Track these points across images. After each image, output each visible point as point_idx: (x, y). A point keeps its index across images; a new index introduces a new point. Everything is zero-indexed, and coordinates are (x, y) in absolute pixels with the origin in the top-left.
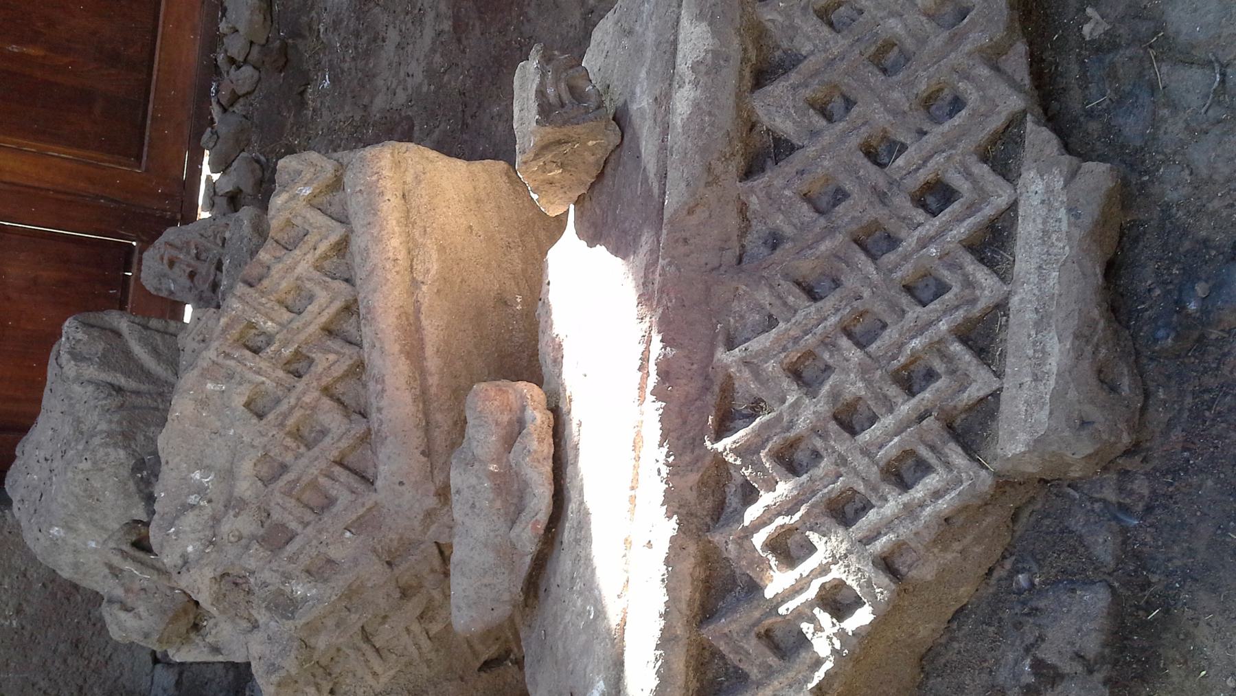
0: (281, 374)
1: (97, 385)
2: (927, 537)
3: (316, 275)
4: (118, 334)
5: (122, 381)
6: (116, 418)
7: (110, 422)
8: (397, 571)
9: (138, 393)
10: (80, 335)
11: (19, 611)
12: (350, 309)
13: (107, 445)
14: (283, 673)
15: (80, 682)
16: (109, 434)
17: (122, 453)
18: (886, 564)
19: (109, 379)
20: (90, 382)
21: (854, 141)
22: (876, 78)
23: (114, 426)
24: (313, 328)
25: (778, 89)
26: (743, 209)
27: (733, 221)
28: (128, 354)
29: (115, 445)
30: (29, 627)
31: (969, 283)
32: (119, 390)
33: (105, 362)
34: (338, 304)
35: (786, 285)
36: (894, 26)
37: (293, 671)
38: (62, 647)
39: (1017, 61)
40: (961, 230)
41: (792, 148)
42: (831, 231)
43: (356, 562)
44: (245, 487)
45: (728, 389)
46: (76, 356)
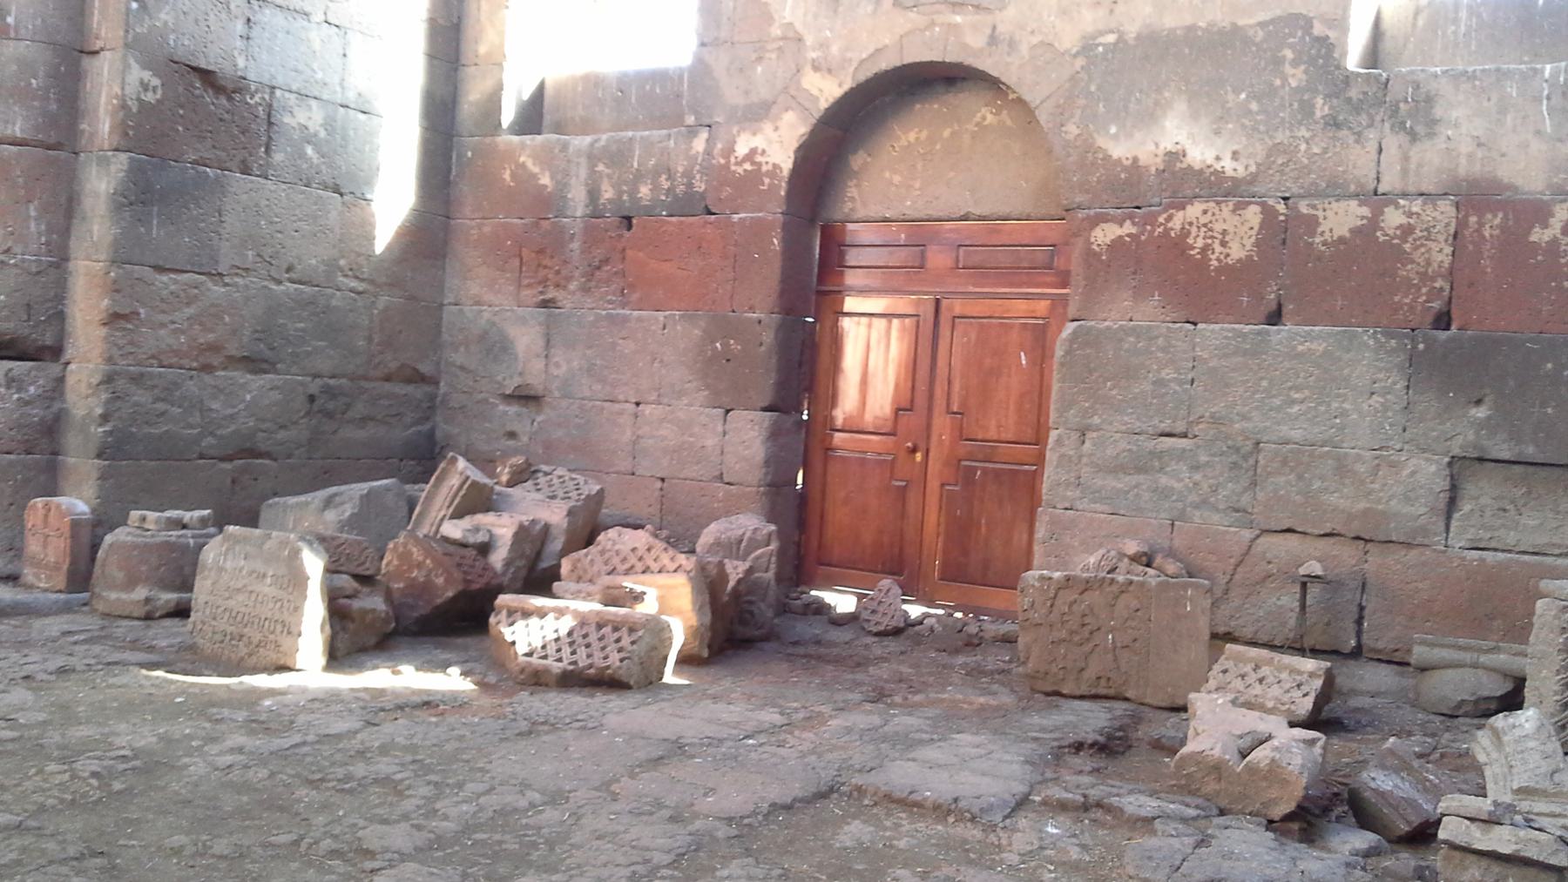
5: (744, 544)
9: (738, 549)
33: (750, 539)
44: (617, 547)
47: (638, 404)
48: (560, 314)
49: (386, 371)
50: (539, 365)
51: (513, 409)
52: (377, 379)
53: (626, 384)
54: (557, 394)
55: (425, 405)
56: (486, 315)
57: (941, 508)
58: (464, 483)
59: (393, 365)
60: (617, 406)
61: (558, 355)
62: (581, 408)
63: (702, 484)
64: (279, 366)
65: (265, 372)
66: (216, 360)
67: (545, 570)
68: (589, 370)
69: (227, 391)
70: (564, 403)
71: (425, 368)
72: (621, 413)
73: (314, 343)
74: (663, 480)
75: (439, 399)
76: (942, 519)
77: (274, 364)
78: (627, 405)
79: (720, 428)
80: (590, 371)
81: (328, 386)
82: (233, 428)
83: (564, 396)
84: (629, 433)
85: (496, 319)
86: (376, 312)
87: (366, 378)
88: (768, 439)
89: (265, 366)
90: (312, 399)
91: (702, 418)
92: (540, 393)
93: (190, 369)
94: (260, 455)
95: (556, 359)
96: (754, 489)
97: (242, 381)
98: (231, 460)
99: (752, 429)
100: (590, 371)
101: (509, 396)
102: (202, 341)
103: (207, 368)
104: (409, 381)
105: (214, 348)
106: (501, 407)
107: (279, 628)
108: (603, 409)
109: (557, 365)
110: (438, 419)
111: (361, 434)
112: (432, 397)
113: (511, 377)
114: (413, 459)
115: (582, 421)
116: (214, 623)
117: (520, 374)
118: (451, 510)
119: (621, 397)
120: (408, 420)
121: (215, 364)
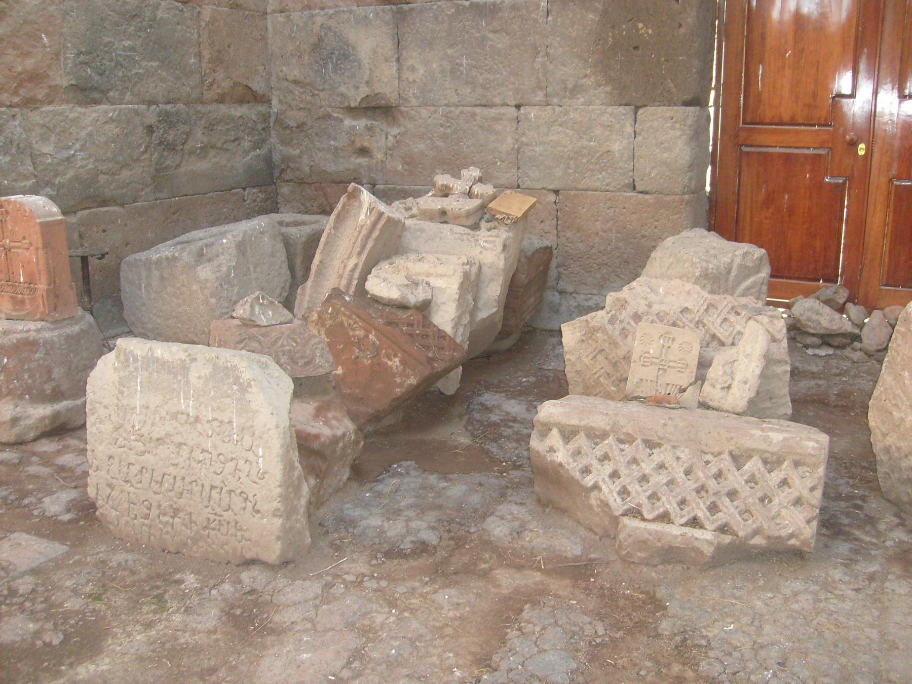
0: (697, 319)
1: (731, 264)
2: (602, 497)
3: (735, 332)
4: (758, 272)
5: (734, 273)
6: (714, 271)
7: (712, 269)
8: (622, 361)
9: (727, 280)
10: (756, 256)
11: (643, 236)
12: (723, 344)
13: (702, 268)
14: (590, 321)
15: (609, 264)
16: (707, 269)
17: (697, 274)
18: (596, 487)
19: (734, 268)
20: (732, 261)
21: (737, 486)
22: (759, 494)
23: (710, 271)
24: (714, 331)
25: (760, 464)
26: (720, 454)
27: (716, 449)
28: (748, 276)
29: (702, 271)
30: (635, 241)
31: (682, 517)
32: (729, 272)
33: (742, 267)
34: (723, 339)
35: (690, 462)
36: (776, 501)
37: (590, 325)
38: (625, 255)
39: (758, 541)
40: (700, 514)
41: (738, 469)
42: (707, 477)
43: (626, 345)
44: (656, 308)
45: (659, 445)
46: (745, 255)
47: (518, 107)
48: (412, 9)
49: (219, 91)
50: (388, 71)
51: (361, 124)
52: (212, 102)
53: (502, 85)
54: (414, 102)
55: (260, 127)
56: (319, 20)
57: (888, 207)
58: (374, 225)
59: (227, 84)
60: (493, 112)
61: (413, 58)
62: (447, 117)
63: (609, 194)
64: (111, 94)
65: (97, 102)
66: (41, 94)
67: (484, 320)
68: (452, 72)
69: (58, 130)
70: (424, 113)
71: (257, 85)
72: (498, 119)
73: (144, 63)
74: (556, 192)
75: (272, 119)
76: (889, 219)
77: (104, 92)
78: (503, 110)
79: (629, 129)
80: (454, 71)
81: (168, 114)
82: (71, 173)
83: (424, 104)
84: (510, 140)
85: (332, 23)
86: (203, 24)
87: (201, 101)
88: (691, 139)
89: (96, 95)
90: (150, 129)
91: (605, 118)
92: (393, 99)
93: (11, 106)
94: (104, 203)
95: (410, 62)
96: (677, 198)
97: (72, 116)
98: (75, 212)
99: (673, 128)
100: (454, 71)
101: (355, 108)
102: (19, 69)
103: (30, 103)
104: (241, 101)
105: (35, 77)
106: (348, 122)
107: (238, 503)
108: (474, 115)
109: (413, 69)
110: (273, 139)
111: (201, 166)
112: (266, 118)
113: (357, 88)
114: (254, 187)
115: (449, 131)
116: (127, 487)
117: (367, 82)
118: (364, 256)
119: (497, 100)
120: (246, 145)
121: (40, 97)
